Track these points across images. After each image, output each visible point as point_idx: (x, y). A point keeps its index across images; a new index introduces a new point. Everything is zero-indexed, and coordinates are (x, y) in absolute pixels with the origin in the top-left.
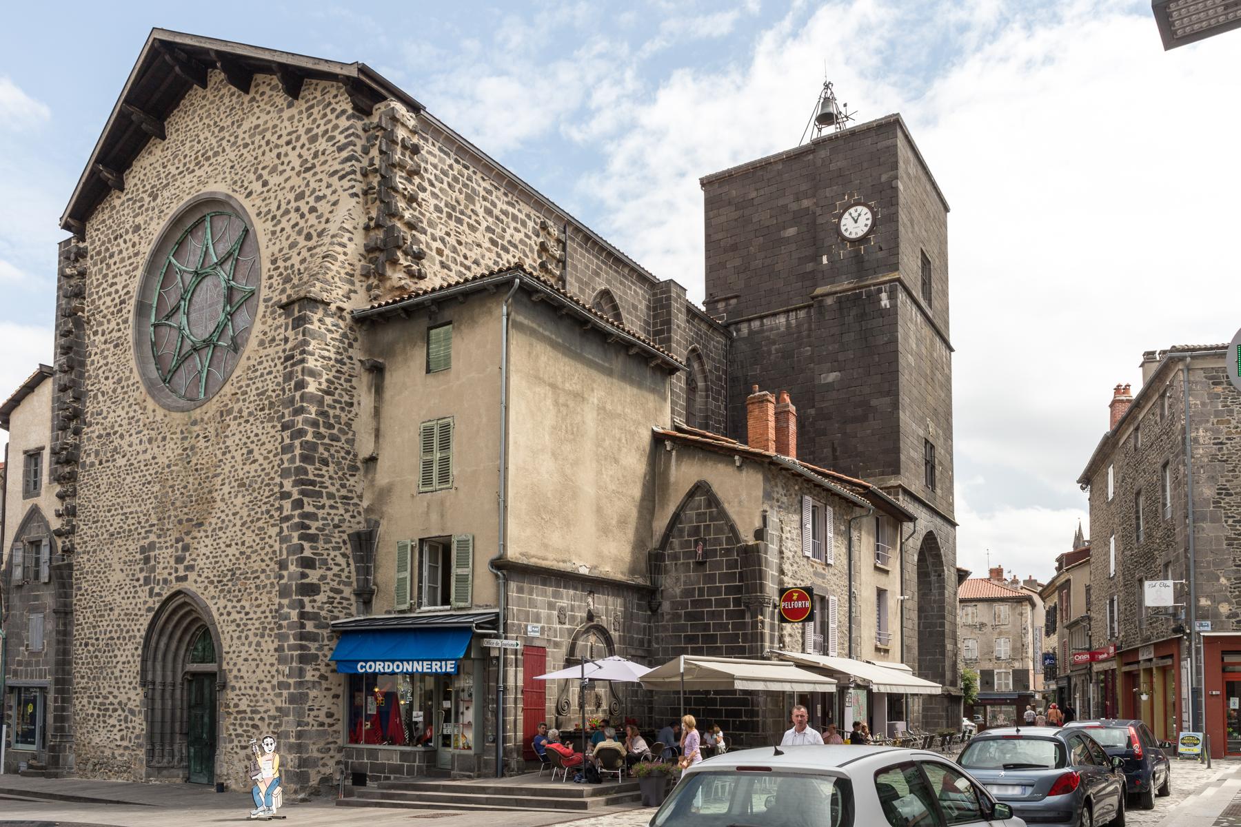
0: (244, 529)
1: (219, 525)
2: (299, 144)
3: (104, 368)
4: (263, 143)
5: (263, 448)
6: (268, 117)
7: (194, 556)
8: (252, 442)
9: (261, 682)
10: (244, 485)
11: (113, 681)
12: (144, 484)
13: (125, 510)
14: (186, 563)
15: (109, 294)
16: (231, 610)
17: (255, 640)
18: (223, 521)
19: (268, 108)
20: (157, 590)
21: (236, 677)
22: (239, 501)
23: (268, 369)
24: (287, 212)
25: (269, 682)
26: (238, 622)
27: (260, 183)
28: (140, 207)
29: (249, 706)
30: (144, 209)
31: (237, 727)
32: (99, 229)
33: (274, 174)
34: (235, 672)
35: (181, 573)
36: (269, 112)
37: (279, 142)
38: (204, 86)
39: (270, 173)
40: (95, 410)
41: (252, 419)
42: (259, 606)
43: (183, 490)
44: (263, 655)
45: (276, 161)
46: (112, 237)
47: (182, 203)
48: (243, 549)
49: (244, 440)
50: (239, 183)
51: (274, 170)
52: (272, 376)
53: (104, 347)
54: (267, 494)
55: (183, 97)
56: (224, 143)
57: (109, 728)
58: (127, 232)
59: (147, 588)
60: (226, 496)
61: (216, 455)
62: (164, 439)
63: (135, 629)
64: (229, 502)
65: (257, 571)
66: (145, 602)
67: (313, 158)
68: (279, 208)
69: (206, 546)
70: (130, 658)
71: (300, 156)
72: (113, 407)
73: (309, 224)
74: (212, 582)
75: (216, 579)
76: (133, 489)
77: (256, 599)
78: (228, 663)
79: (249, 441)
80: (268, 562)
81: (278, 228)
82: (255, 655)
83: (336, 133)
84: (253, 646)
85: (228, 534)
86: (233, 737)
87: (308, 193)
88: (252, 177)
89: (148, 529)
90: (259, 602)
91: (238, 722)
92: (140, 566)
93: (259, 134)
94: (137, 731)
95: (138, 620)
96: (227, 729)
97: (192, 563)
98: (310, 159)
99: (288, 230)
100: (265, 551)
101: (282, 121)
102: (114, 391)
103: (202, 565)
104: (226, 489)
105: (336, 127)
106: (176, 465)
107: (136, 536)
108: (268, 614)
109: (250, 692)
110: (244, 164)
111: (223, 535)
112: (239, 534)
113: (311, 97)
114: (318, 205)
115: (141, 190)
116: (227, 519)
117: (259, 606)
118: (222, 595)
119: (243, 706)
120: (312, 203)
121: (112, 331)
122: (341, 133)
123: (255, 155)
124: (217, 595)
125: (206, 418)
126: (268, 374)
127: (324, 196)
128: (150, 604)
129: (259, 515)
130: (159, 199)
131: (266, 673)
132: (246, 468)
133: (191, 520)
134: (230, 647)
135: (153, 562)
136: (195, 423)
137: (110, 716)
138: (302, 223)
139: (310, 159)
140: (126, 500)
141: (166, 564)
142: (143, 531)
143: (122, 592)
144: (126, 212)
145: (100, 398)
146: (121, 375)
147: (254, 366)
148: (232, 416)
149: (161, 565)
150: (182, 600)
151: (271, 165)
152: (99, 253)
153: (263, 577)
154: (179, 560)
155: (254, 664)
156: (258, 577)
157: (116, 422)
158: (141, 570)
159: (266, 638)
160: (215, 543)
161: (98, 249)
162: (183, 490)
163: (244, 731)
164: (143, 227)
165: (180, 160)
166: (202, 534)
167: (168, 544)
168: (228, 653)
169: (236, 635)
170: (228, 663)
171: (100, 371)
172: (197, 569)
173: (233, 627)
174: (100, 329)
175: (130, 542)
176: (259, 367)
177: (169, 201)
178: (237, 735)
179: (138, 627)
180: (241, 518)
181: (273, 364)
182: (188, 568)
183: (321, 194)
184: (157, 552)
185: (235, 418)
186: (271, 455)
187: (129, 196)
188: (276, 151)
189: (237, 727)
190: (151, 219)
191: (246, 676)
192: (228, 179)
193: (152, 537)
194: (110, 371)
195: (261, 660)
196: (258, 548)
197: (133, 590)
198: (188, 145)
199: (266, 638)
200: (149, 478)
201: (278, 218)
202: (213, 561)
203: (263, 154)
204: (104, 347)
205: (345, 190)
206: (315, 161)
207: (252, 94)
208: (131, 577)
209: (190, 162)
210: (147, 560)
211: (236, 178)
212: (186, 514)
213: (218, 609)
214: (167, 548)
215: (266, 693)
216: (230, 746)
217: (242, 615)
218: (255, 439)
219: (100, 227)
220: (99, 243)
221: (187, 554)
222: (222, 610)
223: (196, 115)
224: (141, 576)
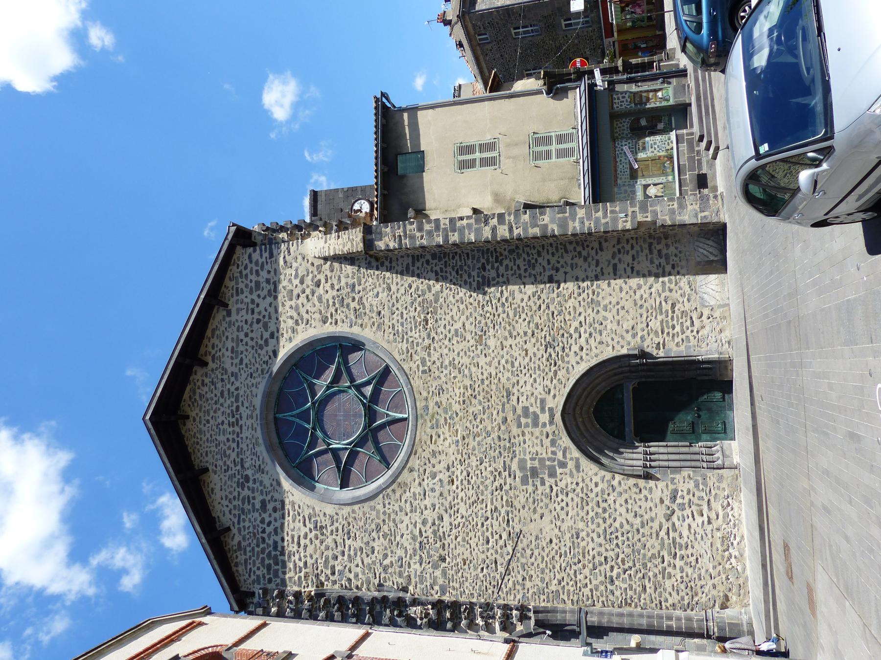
0: (515, 333)
1: (509, 366)
2: (257, 300)
3: (364, 555)
4: (245, 340)
5: (456, 318)
6: (230, 338)
7: (533, 400)
8: (449, 331)
9: (636, 304)
10: (481, 336)
11: (646, 530)
12: (469, 482)
13: (489, 514)
14: (538, 411)
15: (306, 546)
16: (578, 345)
17: (603, 313)
18: (507, 362)
19: (224, 339)
20: (560, 455)
21: (634, 336)
22: (492, 343)
23: (399, 317)
24: (297, 309)
25: (635, 292)
26: (587, 335)
27: (270, 341)
28: (249, 502)
29: (656, 318)
30: (251, 495)
31: (675, 331)
32: (251, 569)
33: (269, 325)
34: (628, 337)
35: (544, 418)
36: (227, 338)
37: (249, 323)
38: (188, 417)
39: (267, 331)
40: (398, 570)
41: (433, 334)
42: (575, 308)
43: (478, 420)
44: (614, 301)
45: (261, 323)
46: (262, 546)
47: (261, 441)
48: (530, 332)
49: (446, 342)
50: (264, 366)
51: (266, 327)
52: (405, 312)
53: (346, 557)
54: (489, 309)
55: (186, 446)
56: (232, 389)
57: (692, 538)
58: (262, 521)
59: (559, 471)
60: (488, 359)
61: (455, 378)
62: (434, 453)
63: (595, 490)
64: (493, 355)
65: (548, 314)
66: (572, 476)
67: (269, 284)
68: (292, 318)
69: (525, 382)
70: (621, 500)
71: (264, 298)
72: (398, 538)
73: (310, 283)
74: (556, 372)
75: (553, 369)
76: (472, 500)
77: (570, 313)
78: (622, 347)
79: (449, 336)
80: (541, 301)
81: (306, 316)
82: (614, 311)
83: (260, 261)
84: (607, 314)
85: (516, 354)
86: (684, 336)
87: (290, 287)
88: (263, 352)
89: (507, 473)
90: (571, 309)
91: (671, 330)
92: (538, 484)
93: (238, 346)
94: (691, 485)
95: (587, 485)
96: (677, 345)
97: (538, 401)
98: (269, 287)
99: (308, 306)
100: (533, 305)
101: (237, 321)
102: (385, 536)
103: (540, 389)
104: (482, 361)
105: (257, 263)
106: (457, 431)
107: (511, 493)
108: (581, 298)
109: (645, 316)
110: (253, 361)
111: (518, 361)
112: (518, 338)
113: (231, 292)
114: (300, 275)
115: (236, 503)
116: (506, 357)
117: (575, 308)
118: (566, 359)
119: (655, 324)
120: (296, 282)
121: (336, 542)
122: (261, 256)
123: (250, 349)
124: (567, 365)
125: (425, 394)
126: (402, 317)
127: (296, 270)
128: (571, 465)
129: (505, 315)
130: (249, 473)
131: (628, 297)
132: (468, 337)
133: (503, 405)
135: (536, 464)
136: (426, 408)
137: (681, 536)
138: (308, 291)
139: (269, 287)
140: (480, 514)
141: (539, 442)
142: (509, 481)
143: (563, 515)
144: (247, 524)
145: (387, 562)
146: (373, 526)
147: (394, 334)
148: (427, 359)
149: (539, 448)
151: (262, 329)
152: (269, 567)
153: (552, 308)
154: (535, 424)
155: (622, 313)
156: (553, 313)
157: (411, 532)
158: (543, 483)
159: (600, 299)
160: (524, 372)
161: (265, 571)
162: (478, 420)
163: (678, 321)
164: (264, 497)
165: (229, 448)
166: (515, 391)
167: (521, 438)
169: (598, 338)
171: (367, 561)
172: (544, 396)
173: (592, 341)
174: (332, 562)
175: (516, 503)
176: (396, 328)
177: (254, 458)
178: (683, 333)
179: (593, 486)
180: (506, 339)
181: (397, 312)
182: (543, 410)
183: (294, 273)
184: (528, 457)
185: (429, 355)
186: (462, 307)
187: (236, 520)
188: (255, 326)
189: (675, 331)
190: (261, 482)
191: (631, 323)
192: (258, 380)
193: (514, 466)
194: (368, 543)
195: (618, 303)
196: (529, 314)
197: (561, 497)
198: (221, 438)
199: (600, 299)
200: (465, 473)
201: (299, 318)
202: (538, 372)
203: (252, 339)
204: (346, 557)
205: (298, 249)
206: (272, 281)
207: (209, 359)
208: (547, 501)
209: (234, 432)
210: (534, 472)
211: (260, 372)
212: (498, 413)
214: (525, 442)
215: (645, 296)
216: (692, 338)
217: (582, 330)
218: (448, 327)
219: (249, 567)
220: (262, 568)
221: (531, 410)
222: (578, 358)
223: (204, 429)
224: (549, 481)
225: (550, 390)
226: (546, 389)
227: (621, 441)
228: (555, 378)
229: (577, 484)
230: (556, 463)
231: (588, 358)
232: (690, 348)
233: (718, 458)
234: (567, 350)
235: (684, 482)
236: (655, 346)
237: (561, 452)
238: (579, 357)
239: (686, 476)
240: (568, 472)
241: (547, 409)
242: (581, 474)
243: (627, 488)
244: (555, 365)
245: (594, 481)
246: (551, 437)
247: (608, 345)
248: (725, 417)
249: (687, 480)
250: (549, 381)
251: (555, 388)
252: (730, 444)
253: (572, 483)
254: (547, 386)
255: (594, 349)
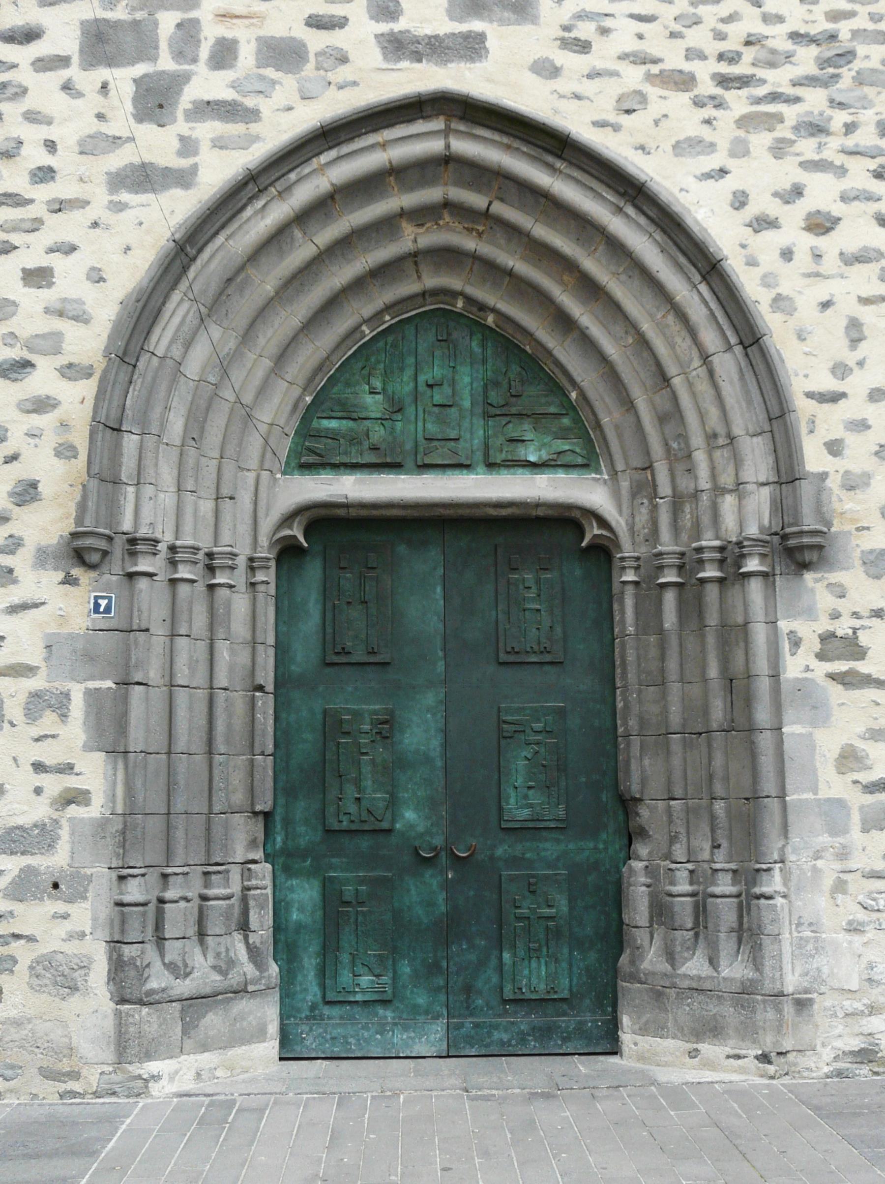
16: (837, 209)
78: (834, 448)
95: (35, 226)
118: (760, 141)
124: (723, 145)
134: (840, 370)
150: (436, 146)
168: (835, 398)
170: (834, 448)
179: (34, 258)
213: (740, 200)
225: (584, 47)
226: (585, 30)
227: (285, 447)
228: (649, 77)
229: (44, 175)
230: (166, 63)
231: (769, 260)
232: (837, 829)
233: (180, 970)
234: (807, 147)
235: (39, 767)
236: (843, 627)
237: (228, 95)
238: (773, 208)
239: (72, 782)
240: (113, 128)
241: (477, 25)
242: (100, 195)
243: (15, 441)
244: (724, 81)
245: (57, 262)
246: (316, 41)
247: (840, 370)
248: (415, 1010)
249: (54, 785)
250: (631, 45)
251: (594, 74)
252: (260, 1035)
253: (51, 146)
254: (604, 31)
255: (822, 291)
